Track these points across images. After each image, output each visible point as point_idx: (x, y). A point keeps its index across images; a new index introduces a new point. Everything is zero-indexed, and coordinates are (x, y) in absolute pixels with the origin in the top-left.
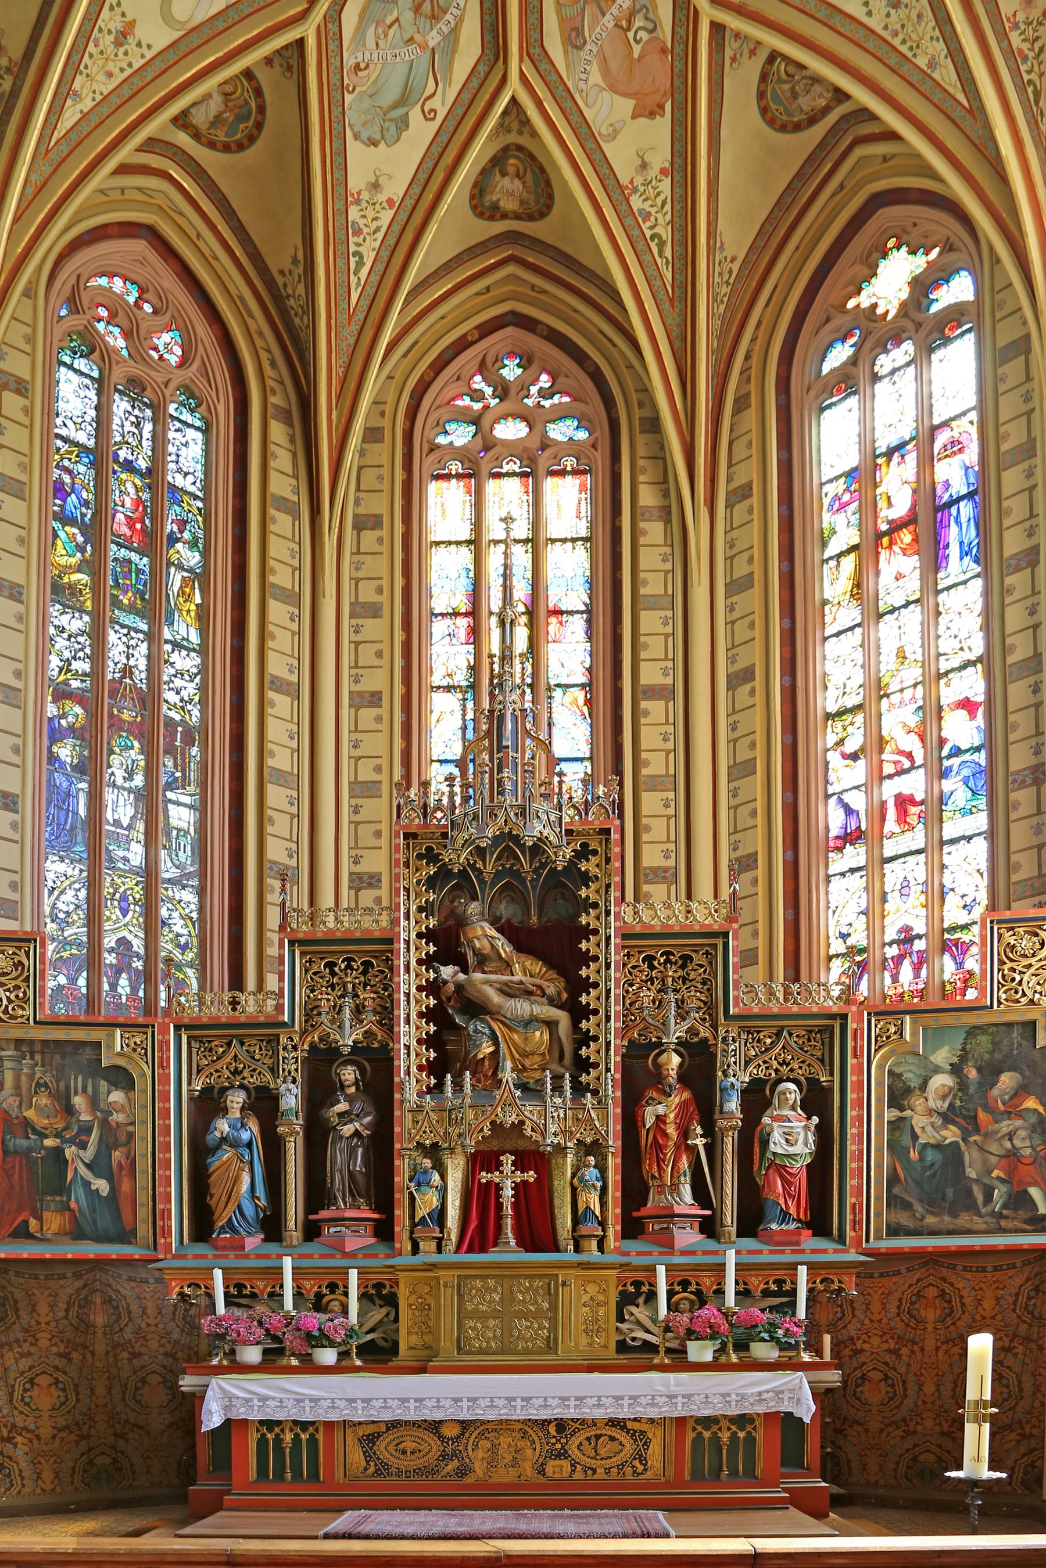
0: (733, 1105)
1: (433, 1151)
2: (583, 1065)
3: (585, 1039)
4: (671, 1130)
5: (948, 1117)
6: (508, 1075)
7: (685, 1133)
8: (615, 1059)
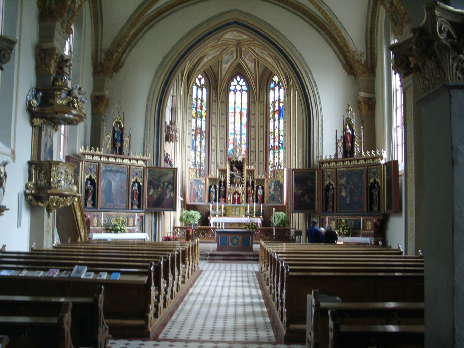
0: (255, 189)
1: (230, 193)
2: (242, 184)
3: (243, 180)
4: (250, 191)
5: (273, 191)
6: (236, 185)
7: (251, 191)
8: (245, 183)
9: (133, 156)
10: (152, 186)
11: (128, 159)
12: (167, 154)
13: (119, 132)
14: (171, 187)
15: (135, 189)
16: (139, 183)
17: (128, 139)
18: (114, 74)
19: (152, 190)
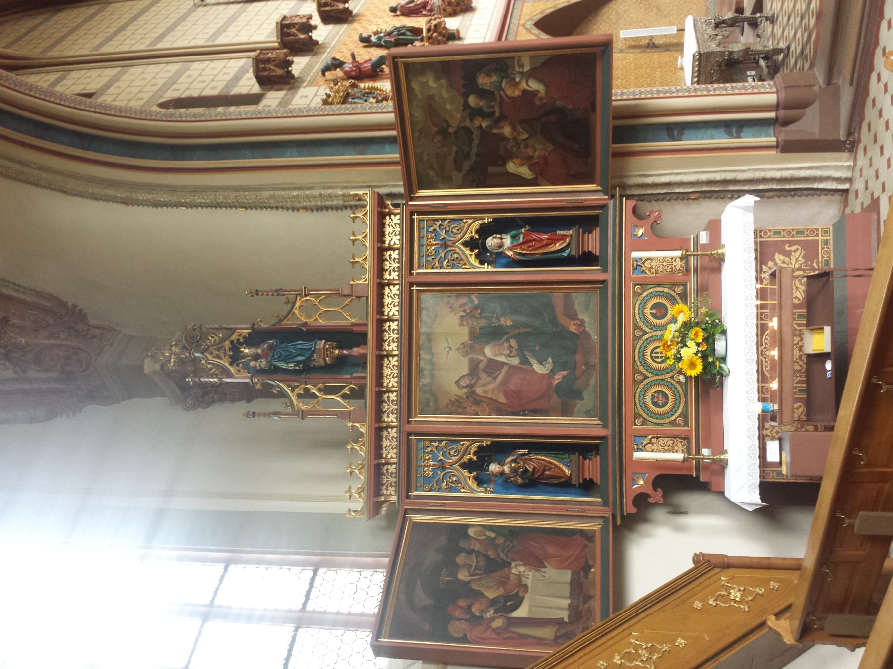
9: (365, 280)
10: (491, 170)
11: (380, 296)
12: (393, 10)
13: (271, 347)
14: (488, 75)
15: (510, 249)
16: (485, 231)
17: (298, 304)
18: (92, 321)
19: (511, 167)
